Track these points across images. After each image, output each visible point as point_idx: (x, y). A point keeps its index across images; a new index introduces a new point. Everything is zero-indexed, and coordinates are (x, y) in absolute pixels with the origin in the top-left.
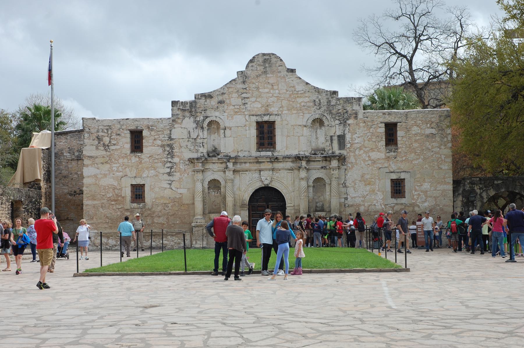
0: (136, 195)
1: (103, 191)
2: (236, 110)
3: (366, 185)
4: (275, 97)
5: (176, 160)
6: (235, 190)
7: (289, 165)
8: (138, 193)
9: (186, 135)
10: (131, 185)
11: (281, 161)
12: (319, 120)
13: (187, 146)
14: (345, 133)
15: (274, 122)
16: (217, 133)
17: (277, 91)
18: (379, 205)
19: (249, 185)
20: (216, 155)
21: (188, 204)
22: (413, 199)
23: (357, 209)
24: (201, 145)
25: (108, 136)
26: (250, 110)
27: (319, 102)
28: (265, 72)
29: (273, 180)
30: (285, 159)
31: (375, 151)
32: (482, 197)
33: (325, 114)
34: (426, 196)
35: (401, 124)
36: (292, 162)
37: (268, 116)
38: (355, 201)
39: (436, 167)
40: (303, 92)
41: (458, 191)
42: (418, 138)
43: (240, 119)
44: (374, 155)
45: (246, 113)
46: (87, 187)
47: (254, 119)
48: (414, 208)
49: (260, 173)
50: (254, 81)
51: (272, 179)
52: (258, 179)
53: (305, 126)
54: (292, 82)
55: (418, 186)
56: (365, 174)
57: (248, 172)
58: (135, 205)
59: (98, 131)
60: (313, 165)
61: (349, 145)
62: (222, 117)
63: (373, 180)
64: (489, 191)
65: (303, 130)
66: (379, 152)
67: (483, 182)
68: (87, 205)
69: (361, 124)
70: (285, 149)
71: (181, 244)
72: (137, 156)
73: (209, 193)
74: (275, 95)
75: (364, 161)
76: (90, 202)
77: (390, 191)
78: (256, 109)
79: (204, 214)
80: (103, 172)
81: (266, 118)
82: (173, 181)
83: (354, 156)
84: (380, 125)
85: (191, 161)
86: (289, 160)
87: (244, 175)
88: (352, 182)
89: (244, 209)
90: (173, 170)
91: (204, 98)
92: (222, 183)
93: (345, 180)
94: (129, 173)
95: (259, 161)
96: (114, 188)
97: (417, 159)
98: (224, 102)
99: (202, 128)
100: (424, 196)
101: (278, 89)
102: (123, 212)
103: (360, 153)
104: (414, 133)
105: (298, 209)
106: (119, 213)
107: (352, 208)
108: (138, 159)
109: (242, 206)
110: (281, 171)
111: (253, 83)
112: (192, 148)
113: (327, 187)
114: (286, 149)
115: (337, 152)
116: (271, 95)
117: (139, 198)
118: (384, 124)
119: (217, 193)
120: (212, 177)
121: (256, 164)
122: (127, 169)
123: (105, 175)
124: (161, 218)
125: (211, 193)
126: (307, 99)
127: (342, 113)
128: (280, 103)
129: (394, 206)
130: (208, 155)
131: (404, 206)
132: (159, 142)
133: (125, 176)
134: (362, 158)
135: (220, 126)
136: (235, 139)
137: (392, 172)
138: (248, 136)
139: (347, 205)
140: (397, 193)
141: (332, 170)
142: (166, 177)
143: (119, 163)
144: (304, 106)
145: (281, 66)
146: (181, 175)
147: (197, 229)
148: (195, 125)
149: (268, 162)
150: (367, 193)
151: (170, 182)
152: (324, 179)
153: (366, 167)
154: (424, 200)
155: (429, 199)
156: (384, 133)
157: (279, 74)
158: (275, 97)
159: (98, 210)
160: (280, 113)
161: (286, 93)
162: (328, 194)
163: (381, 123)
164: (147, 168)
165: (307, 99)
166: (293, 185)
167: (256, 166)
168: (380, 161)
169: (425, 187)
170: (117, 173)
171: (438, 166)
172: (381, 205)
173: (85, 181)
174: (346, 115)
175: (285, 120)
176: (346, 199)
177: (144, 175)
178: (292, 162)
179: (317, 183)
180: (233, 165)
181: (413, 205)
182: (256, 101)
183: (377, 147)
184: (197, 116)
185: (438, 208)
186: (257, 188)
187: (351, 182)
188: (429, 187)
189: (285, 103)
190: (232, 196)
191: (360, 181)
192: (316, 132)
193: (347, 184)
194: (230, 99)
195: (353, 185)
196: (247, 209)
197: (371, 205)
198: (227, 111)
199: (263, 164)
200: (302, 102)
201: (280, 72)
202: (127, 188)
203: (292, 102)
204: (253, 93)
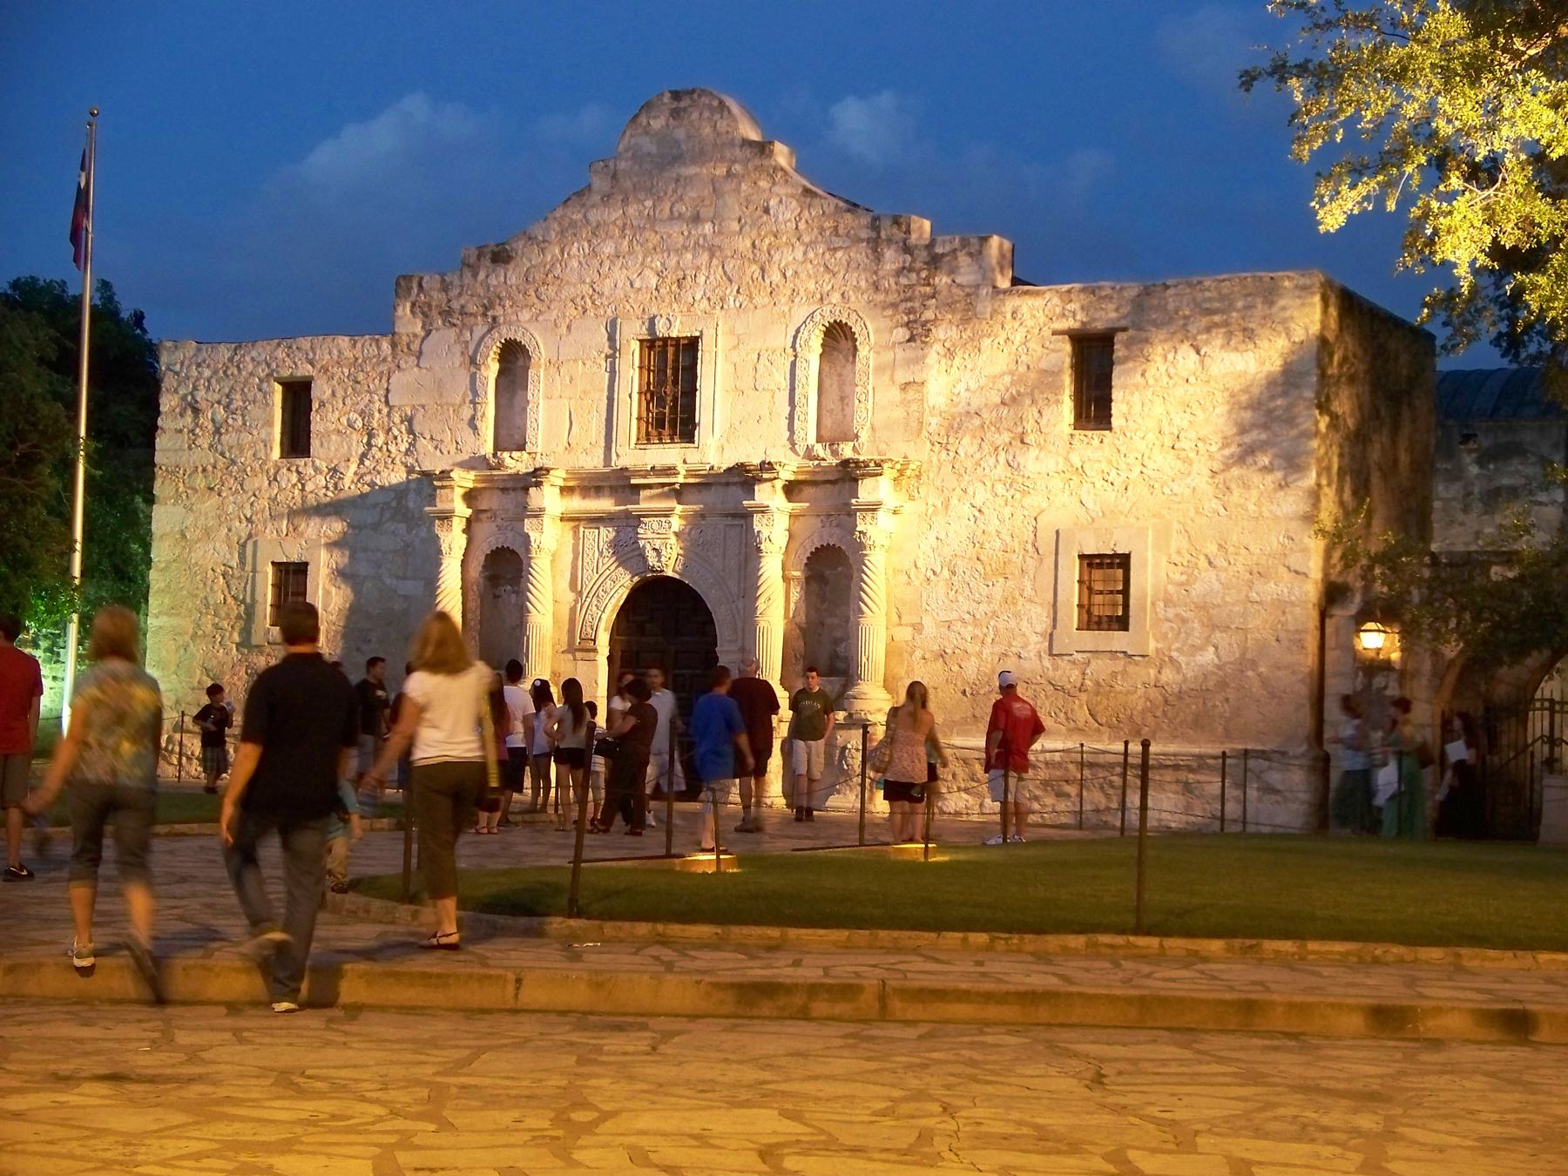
15: (691, 346)
18: (1032, 654)
70: (723, 441)
72: (294, 469)
73: (497, 597)
76: (163, 620)
100: (1196, 625)
108: (294, 478)
125: (505, 596)
131: (1122, 663)
135: (530, 358)
146: (409, 532)
155: (1218, 637)
176: (918, 628)
179: (835, 569)
185: (1250, 673)
187: (938, 563)
192: (840, 375)
195: (946, 573)
197: (1005, 655)
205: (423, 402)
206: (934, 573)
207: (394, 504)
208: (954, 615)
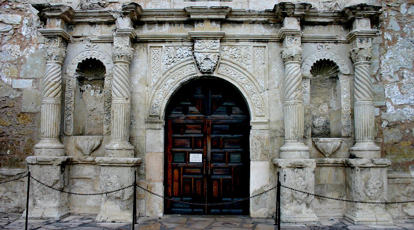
6: (136, 82)
7: (260, 31)
19: (168, 73)
20: (96, 5)
29: (222, 62)
30: (251, 16)
38: (402, 115)
49: (193, 46)
51: (220, 61)
52: (188, 60)
57: (167, 44)
60: (312, 32)
71: (12, 202)
73: (82, 91)
79: (61, 136)
86: (259, 19)
87: (156, 51)
88: (395, 73)
90: (6, 38)
92: (107, 68)
95: (192, 17)
103: (410, 13)
105: (279, 129)
107: (397, 130)
109: (151, 119)
110: (241, 43)
113: (344, 83)
119: (101, 92)
120: (88, 55)
121: (185, 26)
125: (86, 91)
141: (358, 40)
146: (22, 48)
149: (212, 20)
152: (335, 64)
162: (345, 96)
166: (267, 76)
167: (184, 31)
178: (264, 23)
179: (316, 75)
186: (185, 80)
187: (392, 71)
190: (125, 94)
193: (386, 77)
195: (398, 79)
199: (200, 25)
206: (391, 77)
207: (12, 32)
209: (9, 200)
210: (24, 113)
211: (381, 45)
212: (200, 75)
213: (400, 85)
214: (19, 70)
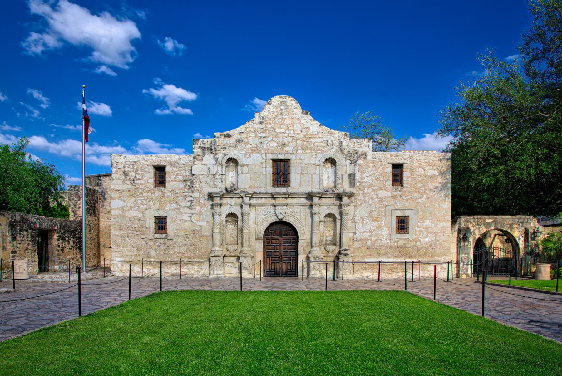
0: (159, 227)
1: (129, 222)
2: (253, 149)
3: (373, 221)
4: (291, 137)
5: (196, 194)
8: (161, 225)
9: (205, 172)
10: (155, 217)
11: (295, 198)
12: (330, 160)
13: (206, 181)
14: (355, 172)
16: (234, 171)
17: (292, 132)
21: (206, 236)
22: (416, 235)
23: (365, 243)
24: (220, 181)
25: (133, 171)
26: (266, 149)
27: (331, 143)
28: (281, 113)
31: (382, 189)
32: (475, 234)
33: (337, 154)
34: (428, 233)
35: (406, 165)
36: (306, 198)
37: (284, 155)
38: (363, 236)
39: (437, 206)
40: (317, 133)
41: (454, 228)
42: (421, 178)
43: (256, 157)
44: (382, 193)
45: (263, 151)
46: (114, 218)
47: (270, 157)
48: (416, 243)
50: (271, 122)
53: (319, 165)
54: (305, 123)
55: (420, 223)
56: (372, 211)
57: (264, 207)
58: (157, 236)
59: (124, 167)
60: (324, 201)
61: (358, 184)
62: (240, 155)
63: (380, 216)
64: (480, 229)
65: (316, 169)
66: (386, 190)
67: (476, 221)
68: (114, 235)
69: (371, 165)
74: (290, 135)
75: (372, 198)
76: (117, 232)
77: (395, 227)
78: (272, 148)
80: (129, 205)
81: (281, 157)
82: (193, 214)
83: (363, 194)
84: (387, 166)
85: (211, 196)
87: (259, 210)
89: (259, 241)
90: (193, 204)
91: (223, 137)
93: (354, 216)
94: (153, 206)
95: (275, 196)
96: (139, 220)
97: (420, 198)
98: (242, 141)
99: (221, 164)
101: (293, 130)
102: (147, 242)
104: (418, 174)
106: (143, 243)
107: (360, 242)
108: (161, 193)
109: (258, 238)
111: (270, 123)
112: (212, 183)
114: (300, 186)
115: (348, 190)
116: (286, 135)
117: (162, 229)
118: (391, 165)
122: (151, 203)
123: (131, 208)
124: (182, 248)
126: (319, 140)
127: (353, 154)
128: (295, 143)
129: (398, 241)
130: (226, 189)
132: (181, 178)
133: (150, 208)
134: (370, 196)
135: (238, 163)
136: (252, 175)
137: (397, 210)
138: (264, 173)
139: (355, 239)
140: (401, 229)
141: (343, 206)
142: (187, 210)
143: (143, 197)
144: (317, 146)
145: (297, 108)
146: (200, 208)
147: (214, 259)
148: (214, 162)
149: (283, 197)
150: (374, 228)
151: (190, 215)
153: (374, 204)
154: (425, 236)
155: (430, 235)
156: (391, 174)
157: (295, 116)
158: (291, 137)
159: (125, 240)
160: (295, 152)
161: (300, 134)
163: (388, 164)
164: (170, 202)
165: (319, 140)
167: (272, 201)
168: (386, 199)
169: (427, 223)
170: (142, 206)
171: (439, 205)
172: (387, 240)
173: (113, 212)
174: (356, 155)
175: (300, 159)
176: (355, 233)
177: (167, 208)
178: (305, 198)
180: (250, 199)
181: (416, 240)
182: (272, 140)
183: (384, 186)
184: (216, 154)
186: (272, 222)
188: (430, 223)
189: (299, 142)
191: (368, 217)
193: (356, 220)
194: (247, 138)
196: (262, 241)
197: (378, 239)
198: (245, 149)
199: (278, 199)
200: (316, 142)
201: (295, 114)
202: (150, 220)
203: (306, 142)
204: (269, 133)
205: (204, 173)
208: (364, 230)
209: (199, 272)
210: (203, 236)
211: (355, 206)
212: (278, 220)
213: (363, 224)
214: (200, 218)
